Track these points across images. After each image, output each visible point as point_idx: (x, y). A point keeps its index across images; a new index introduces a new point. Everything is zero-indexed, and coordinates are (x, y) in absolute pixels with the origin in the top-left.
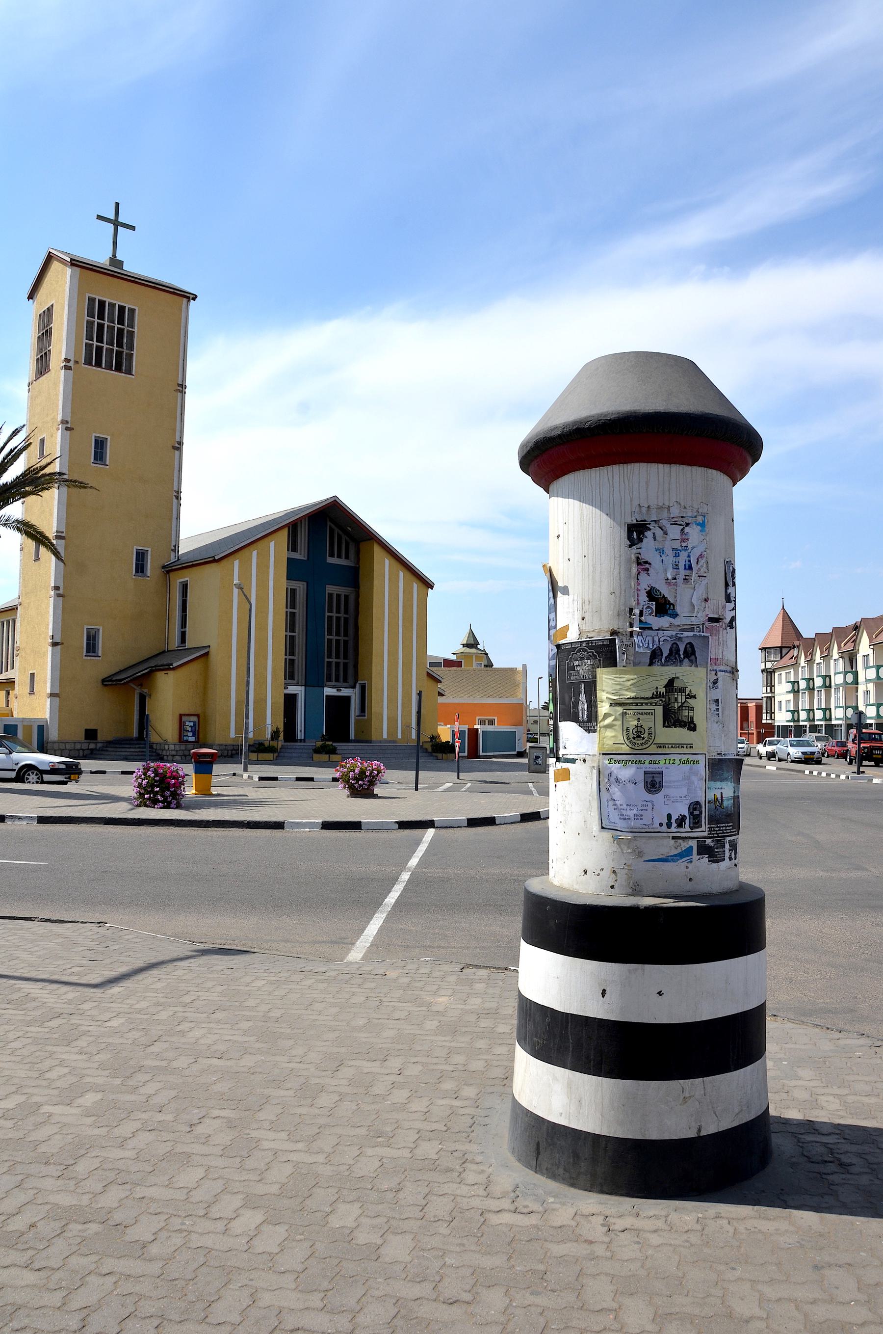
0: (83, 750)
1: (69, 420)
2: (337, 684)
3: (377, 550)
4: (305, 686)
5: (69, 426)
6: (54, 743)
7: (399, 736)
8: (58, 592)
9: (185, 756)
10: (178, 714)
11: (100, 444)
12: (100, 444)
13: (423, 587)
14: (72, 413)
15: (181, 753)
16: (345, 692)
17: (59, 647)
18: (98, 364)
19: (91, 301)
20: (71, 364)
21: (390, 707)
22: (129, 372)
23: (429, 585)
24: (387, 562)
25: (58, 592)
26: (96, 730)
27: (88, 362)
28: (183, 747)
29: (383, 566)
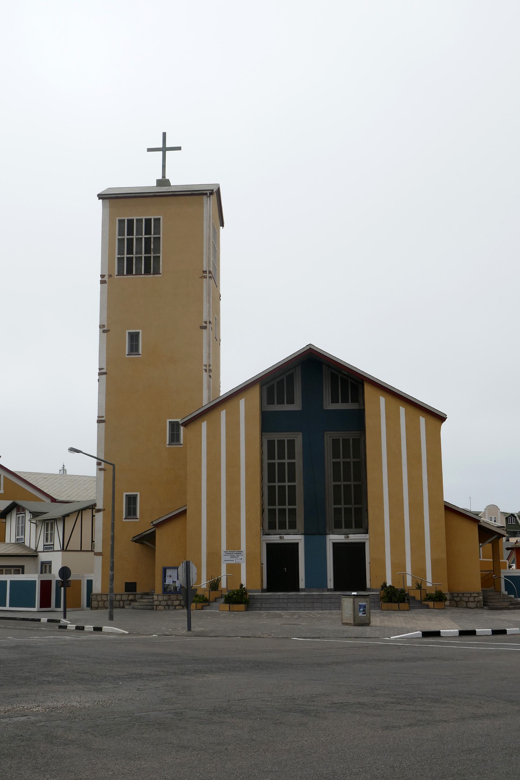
0: (124, 601)
1: (105, 324)
2: (347, 530)
3: (368, 389)
4: (326, 534)
5: (105, 329)
6: (97, 595)
7: (409, 583)
8: (100, 467)
9: (169, 606)
10: (163, 567)
11: (134, 337)
12: (134, 337)
13: (433, 421)
14: (108, 317)
15: (164, 603)
16: (289, 538)
17: (102, 513)
18: (130, 272)
19: (121, 222)
20: (106, 278)
21: (398, 549)
22: (157, 272)
23: (441, 418)
24: (382, 400)
25: (100, 467)
26: (126, 583)
27: (120, 273)
28: (166, 598)
29: (378, 408)
